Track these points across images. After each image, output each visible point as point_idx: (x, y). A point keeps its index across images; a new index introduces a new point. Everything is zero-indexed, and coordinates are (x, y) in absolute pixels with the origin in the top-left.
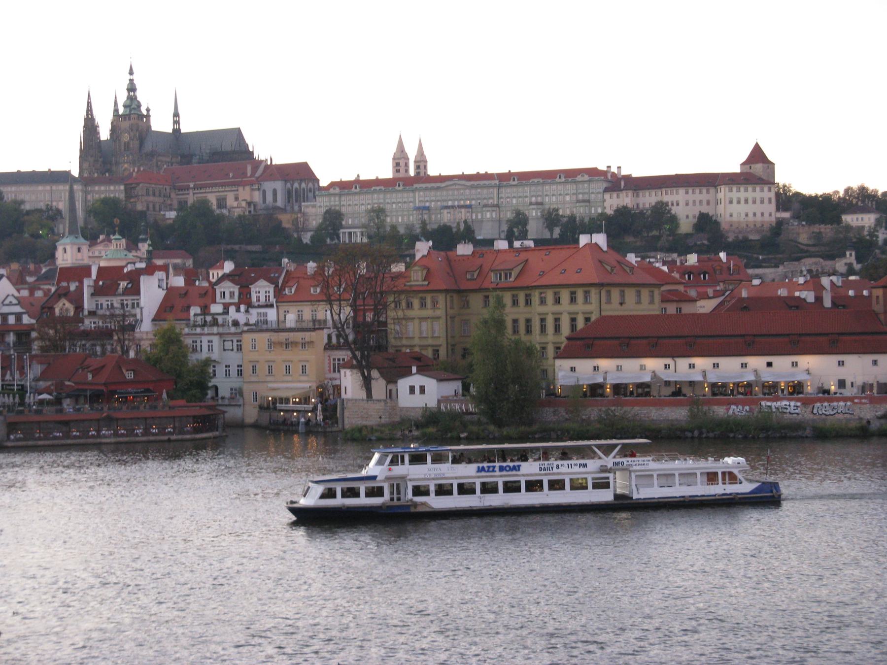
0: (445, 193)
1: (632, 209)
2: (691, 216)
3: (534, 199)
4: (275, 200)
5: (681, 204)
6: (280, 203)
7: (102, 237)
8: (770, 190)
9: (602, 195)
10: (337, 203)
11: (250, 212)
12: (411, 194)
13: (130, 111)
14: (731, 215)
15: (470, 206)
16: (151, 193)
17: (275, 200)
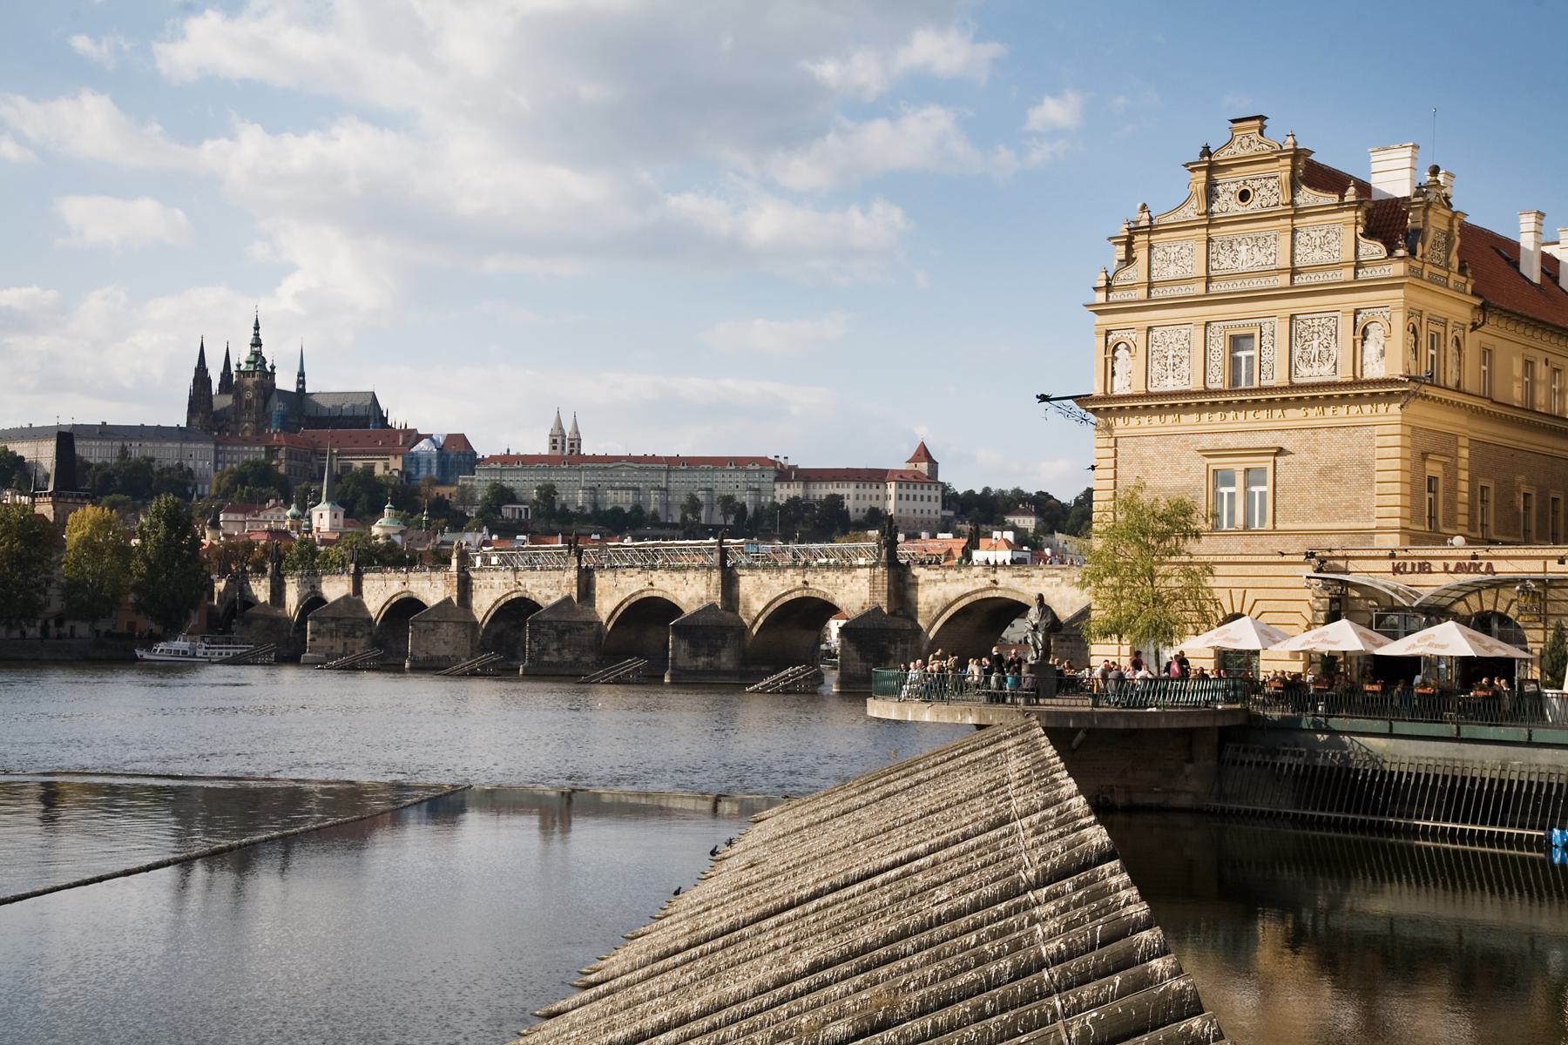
0: (614, 474)
1: (803, 500)
2: (860, 511)
3: (703, 485)
4: (429, 470)
5: (851, 497)
6: (434, 472)
7: (272, 502)
8: (937, 489)
9: (771, 485)
10: (498, 478)
11: (402, 482)
12: (577, 473)
13: (255, 367)
14: (900, 511)
15: (638, 489)
16: (293, 456)
17: (429, 470)
